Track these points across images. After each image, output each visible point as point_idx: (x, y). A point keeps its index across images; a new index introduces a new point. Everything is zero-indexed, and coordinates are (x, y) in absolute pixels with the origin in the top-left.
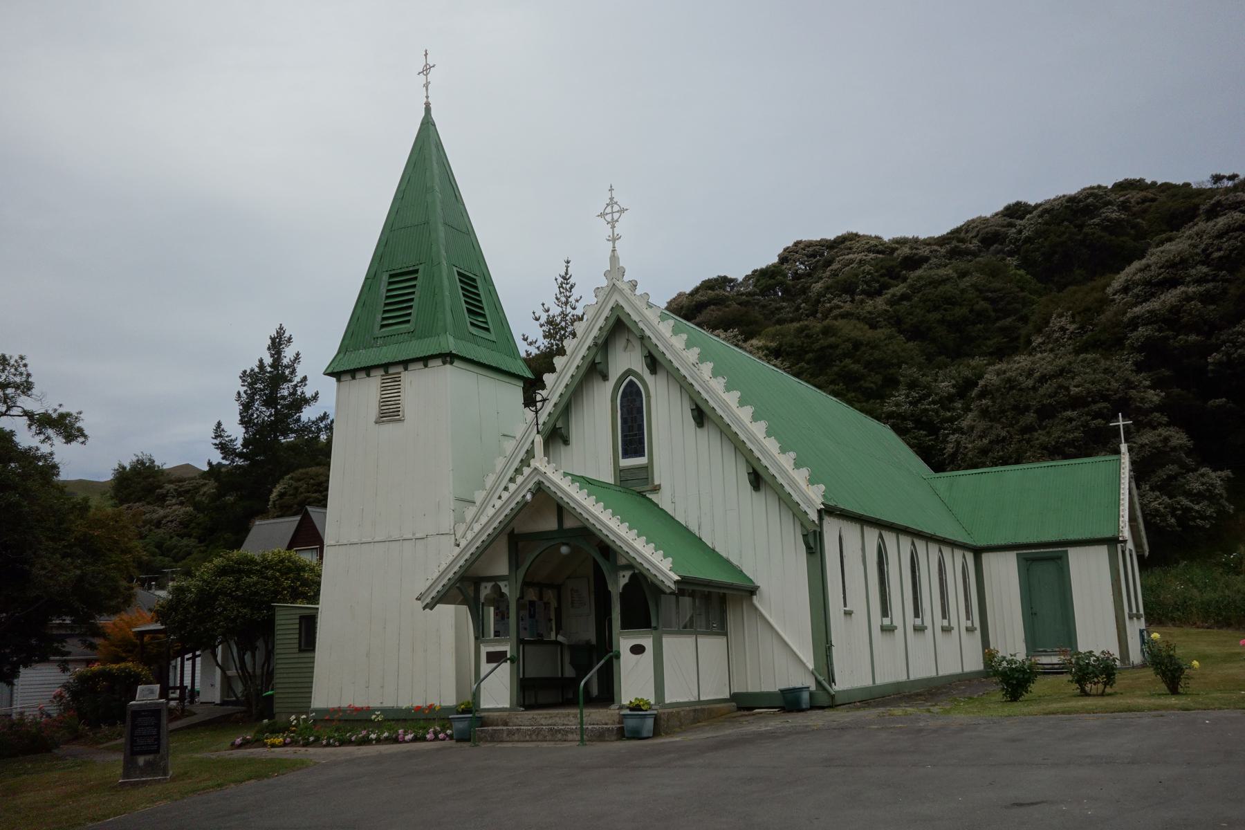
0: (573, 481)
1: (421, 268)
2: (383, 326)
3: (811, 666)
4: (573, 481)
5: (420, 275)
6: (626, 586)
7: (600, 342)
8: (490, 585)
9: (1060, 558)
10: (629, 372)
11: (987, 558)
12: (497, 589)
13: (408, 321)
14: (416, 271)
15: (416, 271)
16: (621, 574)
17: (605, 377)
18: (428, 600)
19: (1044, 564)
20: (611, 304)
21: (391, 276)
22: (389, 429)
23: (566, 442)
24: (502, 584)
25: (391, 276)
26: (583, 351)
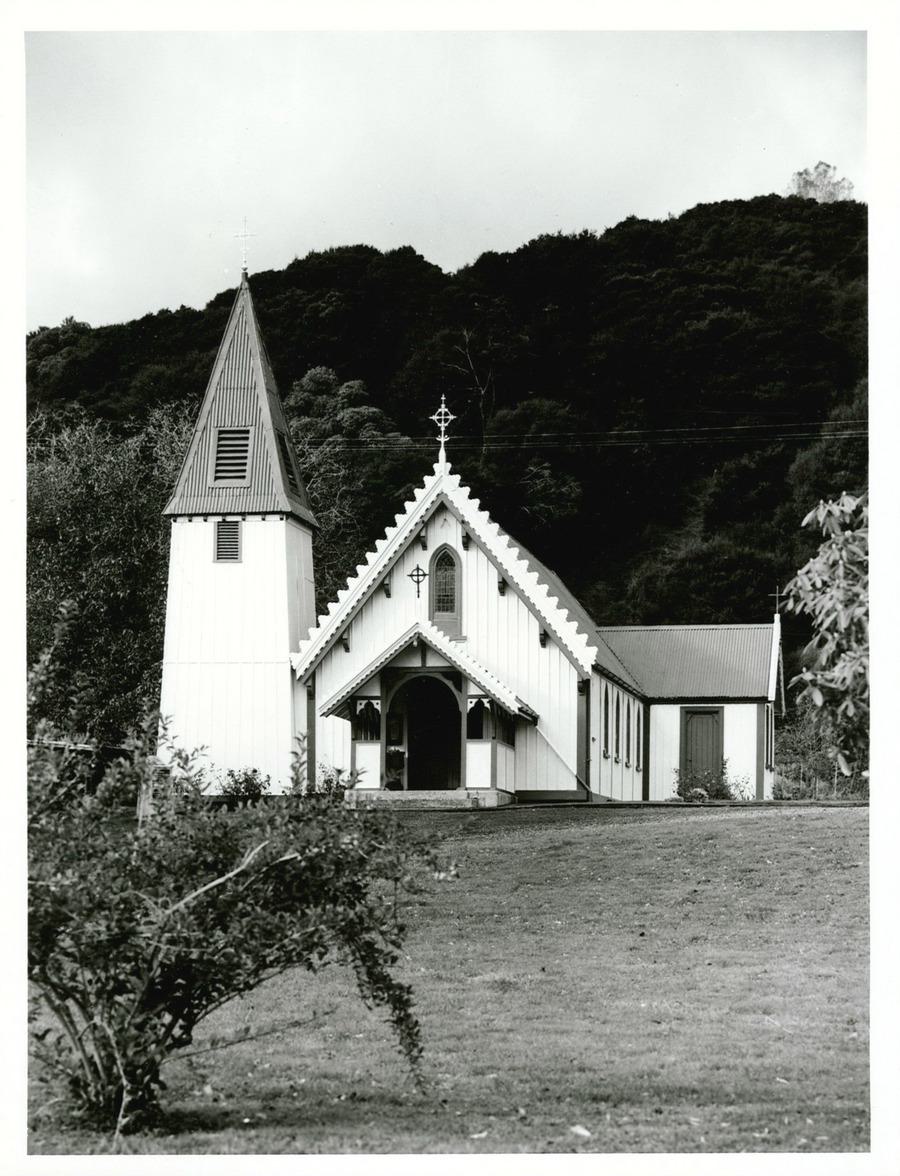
0: (326, 613)
1: (252, 429)
2: (216, 478)
3: (575, 773)
4: (326, 613)
5: (251, 436)
6: (472, 709)
7: (426, 519)
8: (364, 702)
9: (717, 712)
10: (445, 547)
11: (657, 711)
12: (369, 705)
13: (244, 477)
14: (248, 432)
15: (248, 432)
16: (469, 700)
17: (425, 547)
18: (325, 710)
19: (702, 715)
20: (438, 491)
21: (221, 432)
22: (227, 567)
23: (388, 595)
24: (374, 702)
25: (221, 432)
26: (411, 526)
